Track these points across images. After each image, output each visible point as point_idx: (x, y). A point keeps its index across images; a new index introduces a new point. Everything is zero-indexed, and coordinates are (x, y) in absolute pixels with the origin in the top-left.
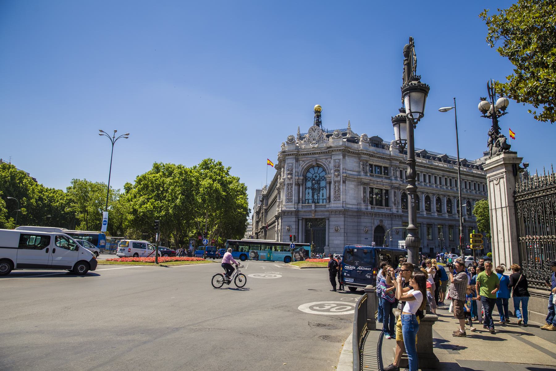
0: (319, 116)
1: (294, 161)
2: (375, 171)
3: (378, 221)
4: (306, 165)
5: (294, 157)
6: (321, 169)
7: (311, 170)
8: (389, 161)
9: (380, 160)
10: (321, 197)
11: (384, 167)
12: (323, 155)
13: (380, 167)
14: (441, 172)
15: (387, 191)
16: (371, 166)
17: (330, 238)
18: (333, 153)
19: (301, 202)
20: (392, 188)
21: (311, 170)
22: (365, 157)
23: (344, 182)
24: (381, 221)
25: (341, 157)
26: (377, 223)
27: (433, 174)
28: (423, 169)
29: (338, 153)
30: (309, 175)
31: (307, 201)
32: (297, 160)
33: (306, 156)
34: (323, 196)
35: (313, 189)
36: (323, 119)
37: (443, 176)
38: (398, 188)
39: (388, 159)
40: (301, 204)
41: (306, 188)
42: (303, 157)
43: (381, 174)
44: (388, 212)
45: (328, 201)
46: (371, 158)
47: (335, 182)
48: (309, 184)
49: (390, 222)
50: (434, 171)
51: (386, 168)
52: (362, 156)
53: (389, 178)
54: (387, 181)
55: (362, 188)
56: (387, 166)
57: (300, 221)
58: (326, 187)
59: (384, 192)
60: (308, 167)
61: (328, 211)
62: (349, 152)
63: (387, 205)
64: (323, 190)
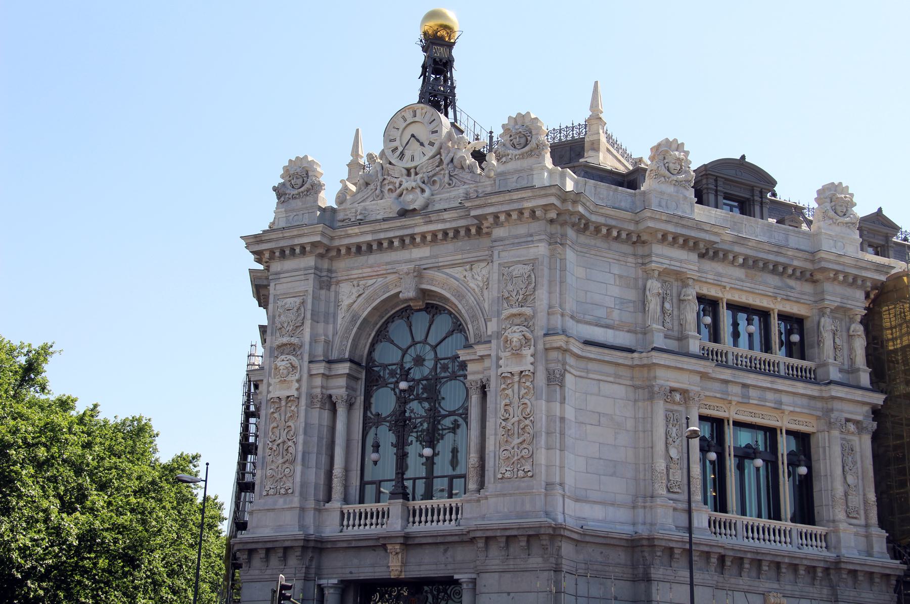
1: (309, 285)
2: (736, 335)
5: (310, 261)
6: (442, 324)
8: (808, 288)
10: (442, 466)
11: (783, 317)
12: (449, 246)
13: (764, 315)
16: (709, 305)
18: (498, 232)
23: (555, 380)
25: (541, 249)
29: (522, 230)
30: (388, 355)
31: (370, 490)
32: (325, 281)
33: (372, 259)
34: (454, 463)
35: (401, 424)
36: (461, 74)
40: (336, 504)
43: (767, 347)
44: (815, 552)
45: (472, 486)
48: (385, 402)
51: (794, 322)
52: (657, 249)
58: (465, 415)
59: (785, 445)
61: (467, 539)
62: (584, 226)
63: (806, 512)
64: (455, 428)
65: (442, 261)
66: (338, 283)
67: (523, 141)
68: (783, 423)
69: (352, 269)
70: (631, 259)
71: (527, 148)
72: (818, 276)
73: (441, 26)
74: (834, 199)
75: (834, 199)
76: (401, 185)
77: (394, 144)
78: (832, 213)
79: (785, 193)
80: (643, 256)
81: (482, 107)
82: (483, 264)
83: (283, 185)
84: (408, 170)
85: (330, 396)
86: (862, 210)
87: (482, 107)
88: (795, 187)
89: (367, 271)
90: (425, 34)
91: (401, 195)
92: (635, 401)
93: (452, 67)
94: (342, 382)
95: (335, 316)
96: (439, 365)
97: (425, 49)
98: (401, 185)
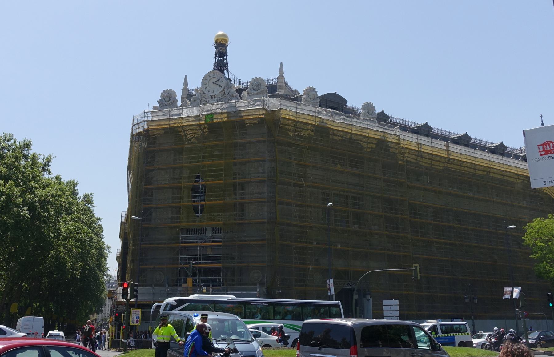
36: (230, 59)
67: (258, 88)
71: (259, 91)
73: (223, 39)
74: (369, 107)
75: (369, 107)
77: (206, 86)
78: (367, 114)
79: (350, 104)
81: (240, 71)
83: (161, 100)
84: (212, 96)
86: (378, 110)
87: (240, 71)
88: (354, 102)
90: (216, 42)
93: (227, 55)
97: (216, 48)
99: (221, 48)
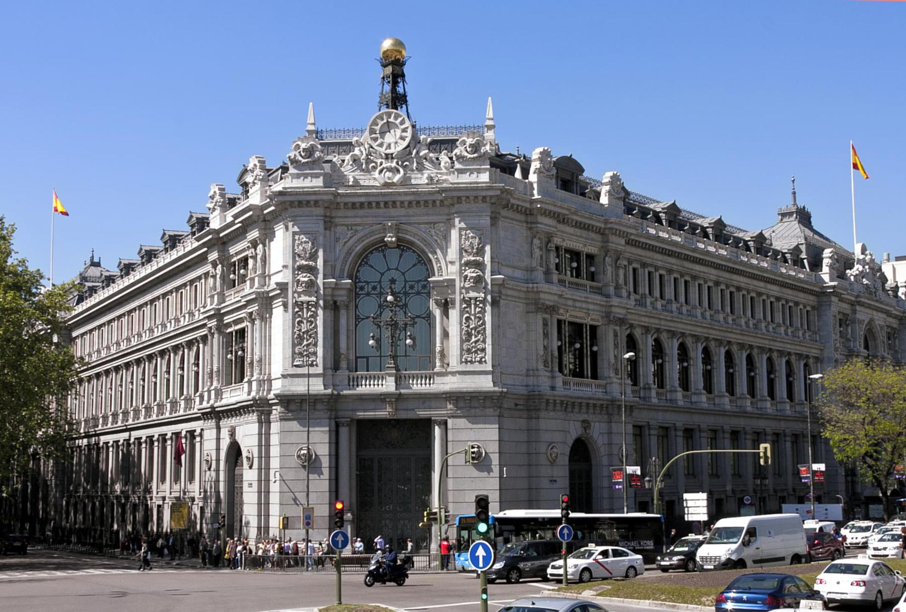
0: (397, 77)
3: (578, 424)
4: (360, 240)
5: (319, 211)
6: (409, 258)
7: (376, 258)
8: (598, 237)
9: (578, 232)
14: (713, 271)
15: (594, 329)
17: (451, 484)
19: (344, 364)
20: (610, 322)
21: (376, 258)
22: (546, 223)
24: (586, 424)
26: (575, 431)
27: (694, 278)
28: (673, 260)
33: (361, 212)
37: (717, 283)
38: (622, 321)
39: (599, 231)
41: (358, 319)
42: (351, 213)
44: (599, 393)
46: (561, 227)
47: (468, 302)
49: (604, 427)
50: (698, 267)
51: (590, 257)
52: (541, 219)
53: (599, 291)
54: (598, 298)
55: (538, 320)
56: (593, 250)
57: (344, 431)
60: (365, 249)
65: (413, 220)
66: (336, 226)
68: (588, 321)
69: (346, 217)
70: (525, 225)
72: (607, 231)
76: (381, 164)
80: (531, 223)
82: (441, 225)
84: (387, 155)
85: (335, 302)
89: (358, 220)
91: (381, 172)
92: (527, 312)
94: (343, 292)
95: (335, 248)
96: (407, 286)
98: (381, 164)
99: (395, 67)
